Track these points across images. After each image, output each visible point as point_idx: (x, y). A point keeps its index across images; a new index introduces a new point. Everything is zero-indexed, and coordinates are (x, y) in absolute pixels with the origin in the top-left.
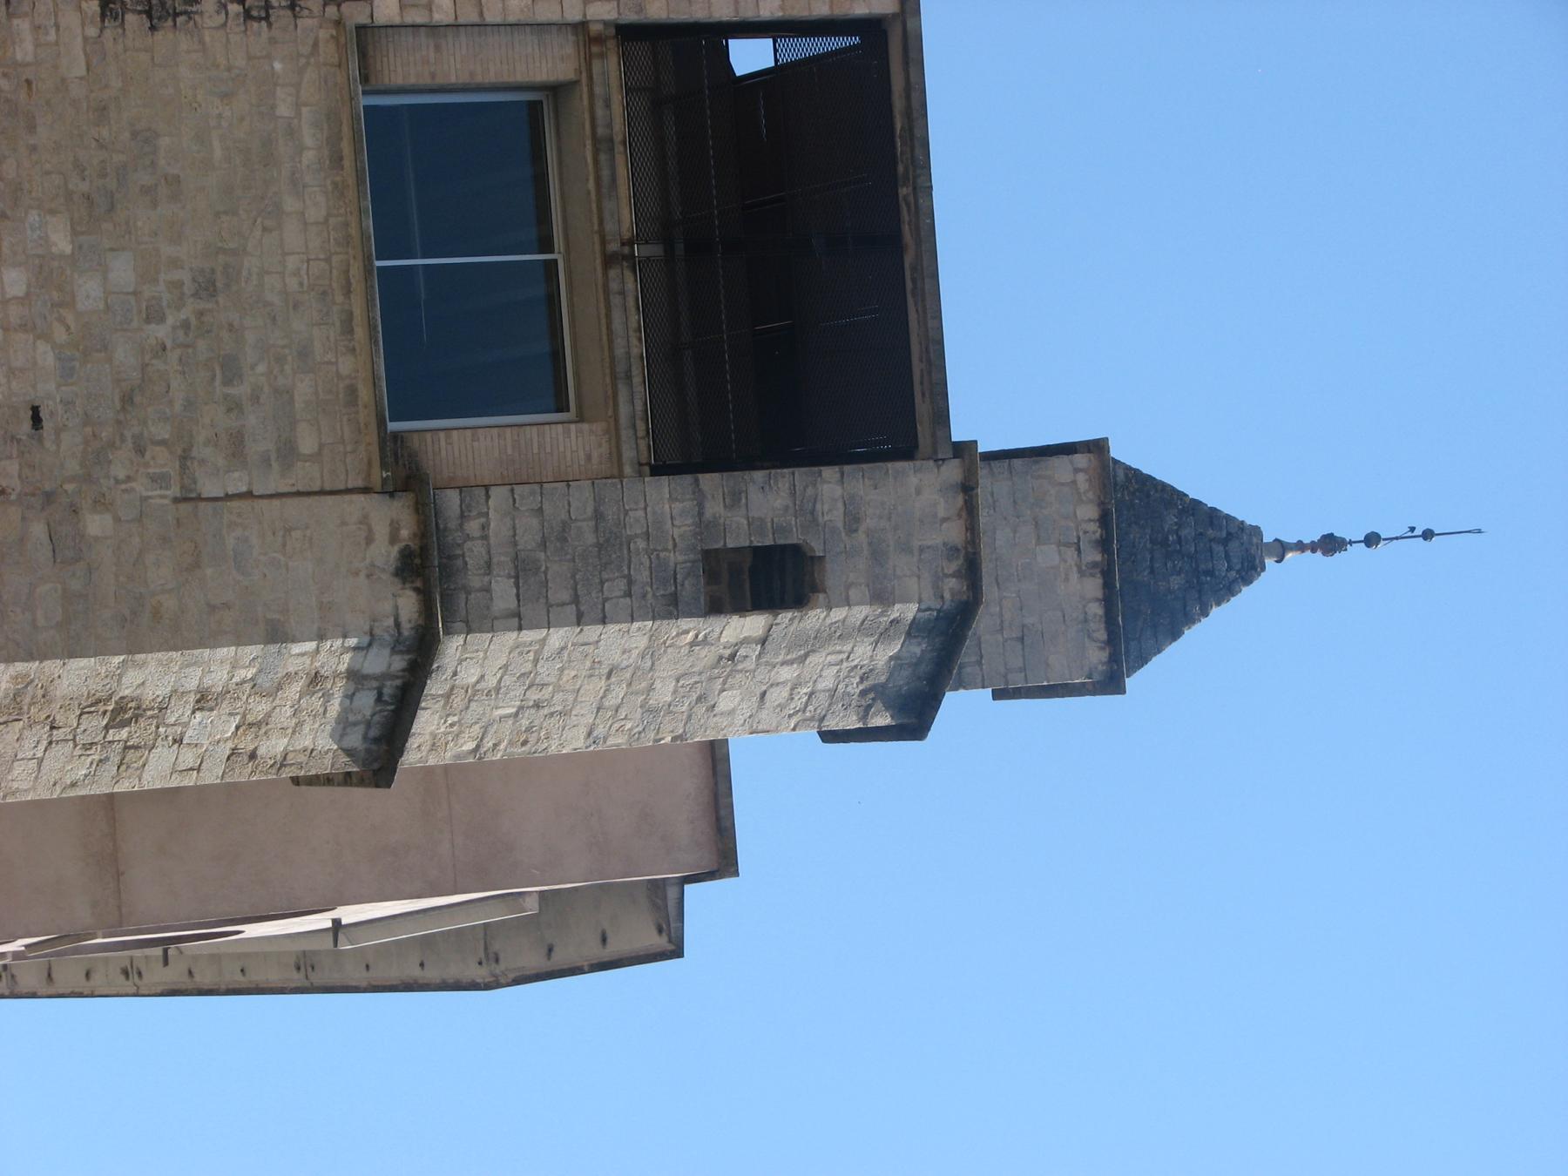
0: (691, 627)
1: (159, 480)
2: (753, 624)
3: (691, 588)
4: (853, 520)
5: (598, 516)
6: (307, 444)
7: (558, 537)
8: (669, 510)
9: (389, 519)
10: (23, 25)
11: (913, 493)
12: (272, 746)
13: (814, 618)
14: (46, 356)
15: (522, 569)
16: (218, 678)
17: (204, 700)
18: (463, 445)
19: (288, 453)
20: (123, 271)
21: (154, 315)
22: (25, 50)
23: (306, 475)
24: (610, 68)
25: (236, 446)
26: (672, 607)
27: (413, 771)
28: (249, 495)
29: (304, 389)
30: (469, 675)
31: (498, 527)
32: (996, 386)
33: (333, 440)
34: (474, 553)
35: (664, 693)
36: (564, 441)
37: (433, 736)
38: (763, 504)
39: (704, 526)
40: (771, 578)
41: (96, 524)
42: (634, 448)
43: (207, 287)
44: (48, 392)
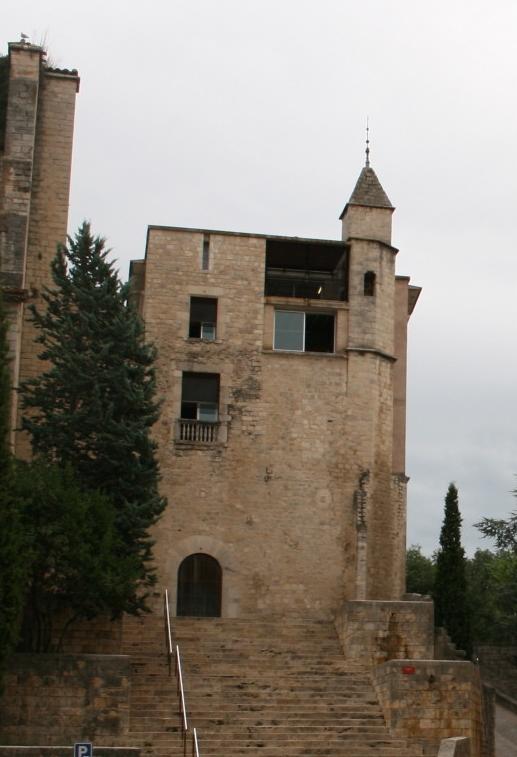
0: (378, 301)
1: (343, 399)
2: (378, 287)
3: (371, 298)
4: (361, 264)
5: (356, 315)
6: (338, 371)
7: (359, 325)
8: (356, 300)
9: (353, 358)
10: (260, 414)
11: (357, 250)
12: (388, 381)
13: (377, 274)
14: (319, 418)
15: (365, 333)
16: (377, 393)
17: (381, 396)
18: (340, 339)
19: (340, 375)
20: (305, 401)
21: (313, 397)
22: (265, 414)
23: (344, 372)
24: (274, 300)
25: (337, 384)
26: (374, 303)
27: (396, 352)
28: (347, 383)
29: (328, 370)
30: (381, 344)
31: (356, 336)
32: (333, 233)
33: (338, 367)
34: (360, 341)
35: (387, 304)
36: (341, 319)
37: (389, 351)
38: (356, 282)
39: (359, 294)
40: (370, 279)
41: (349, 413)
42: (343, 305)
43: (309, 386)
44: (326, 418)
